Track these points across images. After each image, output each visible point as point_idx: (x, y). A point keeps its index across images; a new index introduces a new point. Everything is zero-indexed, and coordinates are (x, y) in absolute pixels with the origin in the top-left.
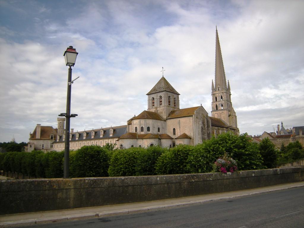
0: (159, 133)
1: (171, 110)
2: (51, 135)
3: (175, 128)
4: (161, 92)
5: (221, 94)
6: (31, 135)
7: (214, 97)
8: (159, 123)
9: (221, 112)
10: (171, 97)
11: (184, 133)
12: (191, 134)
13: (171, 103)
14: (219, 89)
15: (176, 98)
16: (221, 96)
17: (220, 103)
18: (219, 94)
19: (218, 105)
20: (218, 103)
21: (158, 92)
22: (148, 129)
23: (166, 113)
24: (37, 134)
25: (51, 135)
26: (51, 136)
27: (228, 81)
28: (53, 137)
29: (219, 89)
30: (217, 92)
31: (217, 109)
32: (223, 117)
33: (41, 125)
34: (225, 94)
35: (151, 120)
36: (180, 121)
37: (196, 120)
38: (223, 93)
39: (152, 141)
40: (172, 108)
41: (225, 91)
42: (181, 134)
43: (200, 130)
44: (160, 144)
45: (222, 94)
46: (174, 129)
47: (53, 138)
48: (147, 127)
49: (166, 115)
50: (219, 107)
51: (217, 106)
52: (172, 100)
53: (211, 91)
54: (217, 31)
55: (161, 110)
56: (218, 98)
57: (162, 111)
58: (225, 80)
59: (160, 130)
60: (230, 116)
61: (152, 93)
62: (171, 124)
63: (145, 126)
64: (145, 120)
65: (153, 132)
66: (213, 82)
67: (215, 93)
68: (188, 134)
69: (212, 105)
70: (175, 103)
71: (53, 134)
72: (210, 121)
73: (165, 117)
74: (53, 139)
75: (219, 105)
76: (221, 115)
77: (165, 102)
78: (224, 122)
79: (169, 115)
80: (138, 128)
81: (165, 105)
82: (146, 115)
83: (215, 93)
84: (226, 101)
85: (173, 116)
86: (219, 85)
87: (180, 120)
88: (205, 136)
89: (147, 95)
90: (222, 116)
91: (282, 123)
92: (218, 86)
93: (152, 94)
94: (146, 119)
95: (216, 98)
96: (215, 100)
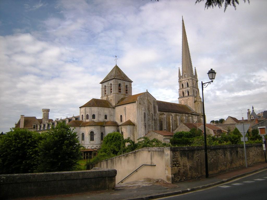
0: (106, 120)
1: (122, 97)
2: (33, 125)
3: (122, 115)
4: (111, 79)
5: (187, 81)
6: (16, 124)
7: (180, 84)
8: (106, 111)
9: (187, 98)
10: (122, 85)
11: (129, 120)
12: (134, 120)
13: (122, 91)
14: (186, 76)
15: (128, 86)
16: (187, 83)
17: (186, 89)
18: (186, 81)
19: (184, 92)
22: (94, 116)
23: (115, 101)
24: (21, 124)
25: (33, 125)
26: (34, 125)
27: (195, 68)
28: (36, 126)
29: (185, 76)
30: (183, 79)
31: (184, 96)
32: (189, 102)
33: (25, 116)
34: (190, 80)
35: (97, 107)
36: (125, 107)
37: (139, 106)
38: (188, 79)
39: (92, 128)
40: (122, 96)
41: (191, 78)
42: (127, 121)
43: (143, 116)
44: (104, 131)
45: (188, 80)
46: (121, 116)
47: (35, 127)
48: (92, 114)
49: (115, 102)
51: (183, 93)
52: (123, 87)
53: (178, 78)
54: (183, 20)
55: (111, 97)
57: (112, 98)
58: (192, 67)
59: (108, 117)
60: (196, 102)
62: (119, 110)
63: (90, 114)
64: (90, 107)
65: (98, 119)
66: (179, 70)
67: (181, 80)
68: (132, 120)
69: (179, 92)
70: (127, 91)
71: (35, 124)
72: (157, 107)
73: (114, 104)
74: (35, 128)
75: (185, 91)
76: (187, 101)
77: (114, 89)
78: (190, 108)
79: (119, 102)
80: (84, 116)
81: (114, 92)
82: (93, 103)
84: (192, 88)
85: (121, 103)
86: (185, 72)
87: (126, 107)
88: (150, 122)
89: (100, 83)
90: (188, 102)
91: (253, 107)
92: (185, 73)
94: (92, 107)
95: (183, 85)
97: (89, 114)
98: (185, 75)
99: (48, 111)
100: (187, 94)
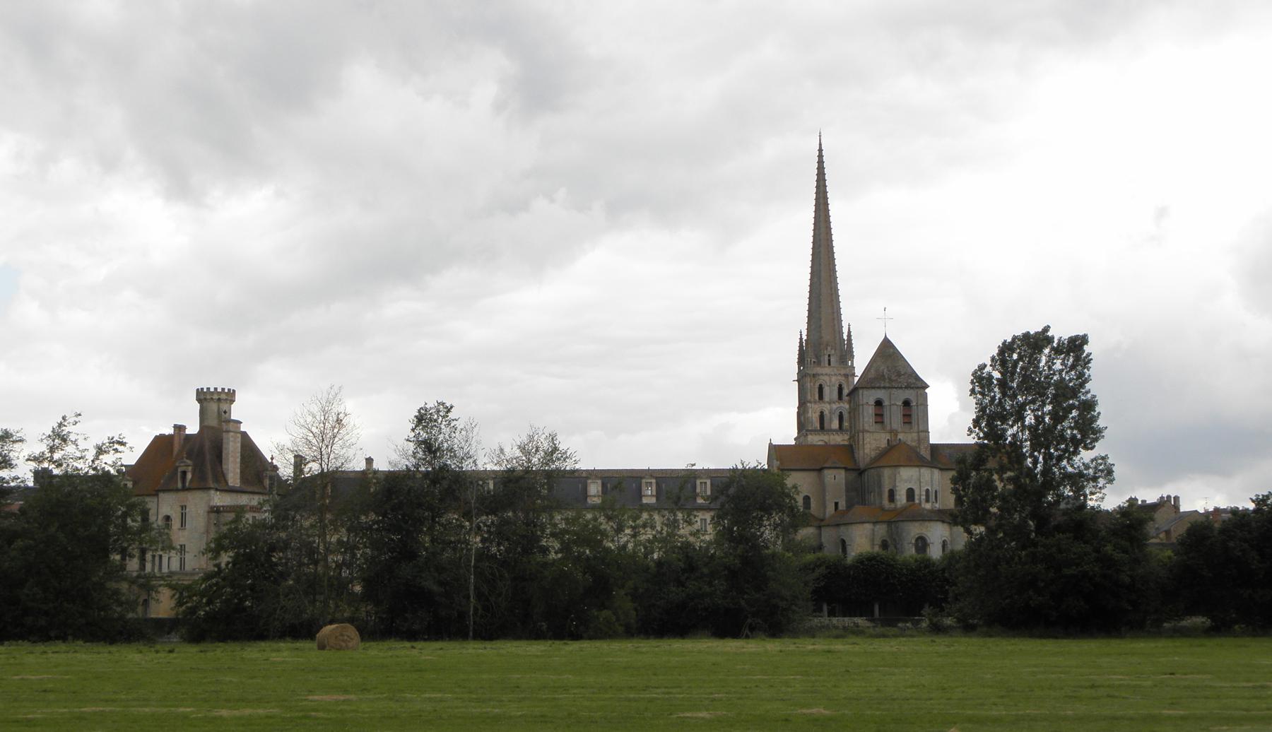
5: (839, 378)
17: (834, 406)
18: (834, 379)
19: (826, 413)
20: (826, 408)
21: (901, 388)
29: (829, 360)
30: (827, 370)
45: (843, 378)
56: (826, 390)
61: (878, 385)
83: (818, 370)
93: (879, 388)
95: (821, 389)
96: (817, 397)
97: (930, 489)
98: (829, 356)
99: (230, 396)
100: (835, 425)
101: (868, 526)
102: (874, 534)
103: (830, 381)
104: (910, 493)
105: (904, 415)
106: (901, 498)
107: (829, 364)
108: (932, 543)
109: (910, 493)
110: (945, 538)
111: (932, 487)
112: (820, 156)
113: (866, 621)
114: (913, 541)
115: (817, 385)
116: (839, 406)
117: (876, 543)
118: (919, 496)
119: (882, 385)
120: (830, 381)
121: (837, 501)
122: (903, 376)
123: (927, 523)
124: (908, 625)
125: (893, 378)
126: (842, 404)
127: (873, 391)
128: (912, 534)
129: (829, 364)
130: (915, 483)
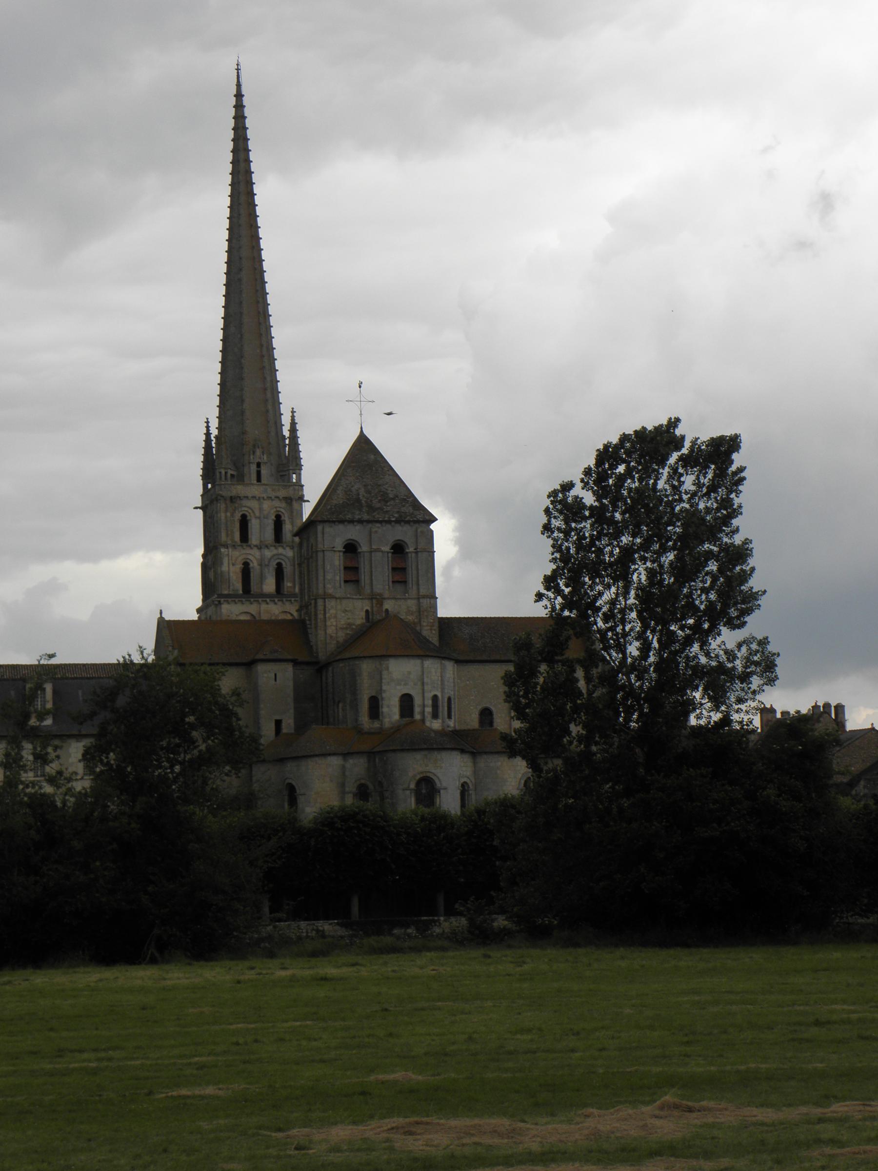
3: (493, 709)
5: (277, 503)
14: (264, 471)
17: (268, 553)
18: (266, 505)
19: (254, 564)
20: (254, 556)
21: (389, 522)
29: (259, 474)
30: (255, 490)
45: (284, 505)
50: (262, 578)
54: (239, 96)
56: (254, 525)
61: (349, 516)
83: (239, 490)
93: (351, 522)
97: (439, 695)
98: (259, 465)
100: (270, 585)
101: (335, 761)
102: (344, 774)
103: (261, 509)
104: (407, 702)
105: (394, 569)
106: (391, 712)
107: (259, 479)
108: (445, 789)
109: (407, 702)
110: (465, 780)
111: (442, 692)
112: (239, 107)
113: (337, 927)
114: (413, 786)
115: (238, 516)
116: (275, 552)
117: (347, 789)
118: (422, 707)
119: (357, 517)
120: (261, 509)
121: (278, 718)
122: (392, 502)
123: (436, 755)
124: (409, 931)
125: (376, 504)
126: (281, 550)
127: (341, 527)
128: (411, 774)
129: (259, 479)
130: (415, 684)
